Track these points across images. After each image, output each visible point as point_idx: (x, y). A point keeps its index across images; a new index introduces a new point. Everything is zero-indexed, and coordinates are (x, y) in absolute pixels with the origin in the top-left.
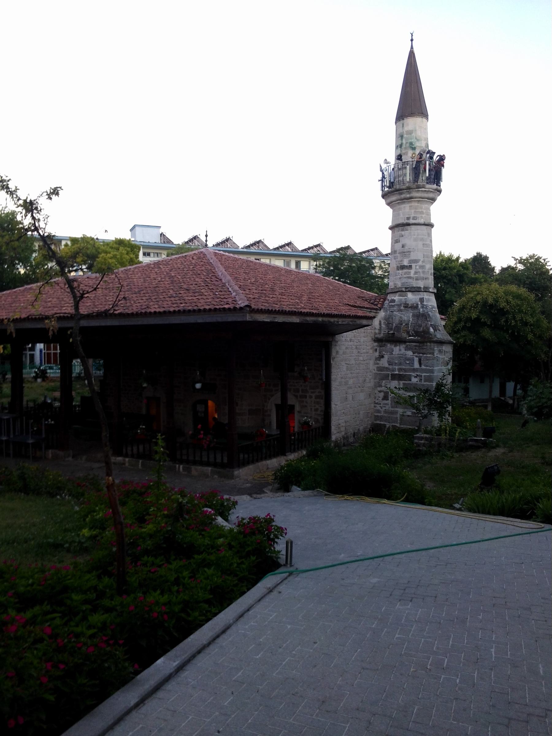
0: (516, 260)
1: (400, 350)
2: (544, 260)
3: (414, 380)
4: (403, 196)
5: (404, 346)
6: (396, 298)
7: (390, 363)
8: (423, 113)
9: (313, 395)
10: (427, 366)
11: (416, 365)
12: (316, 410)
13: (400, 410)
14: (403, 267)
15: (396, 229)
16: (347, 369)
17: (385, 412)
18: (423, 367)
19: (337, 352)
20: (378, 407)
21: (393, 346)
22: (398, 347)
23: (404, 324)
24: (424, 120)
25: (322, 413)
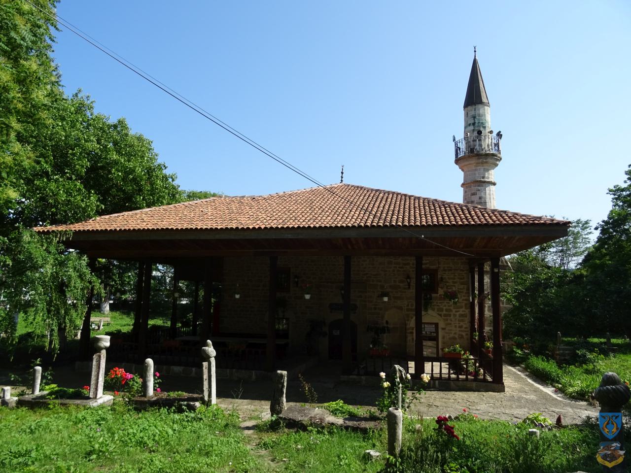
9: (458, 314)
12: (461, 327)
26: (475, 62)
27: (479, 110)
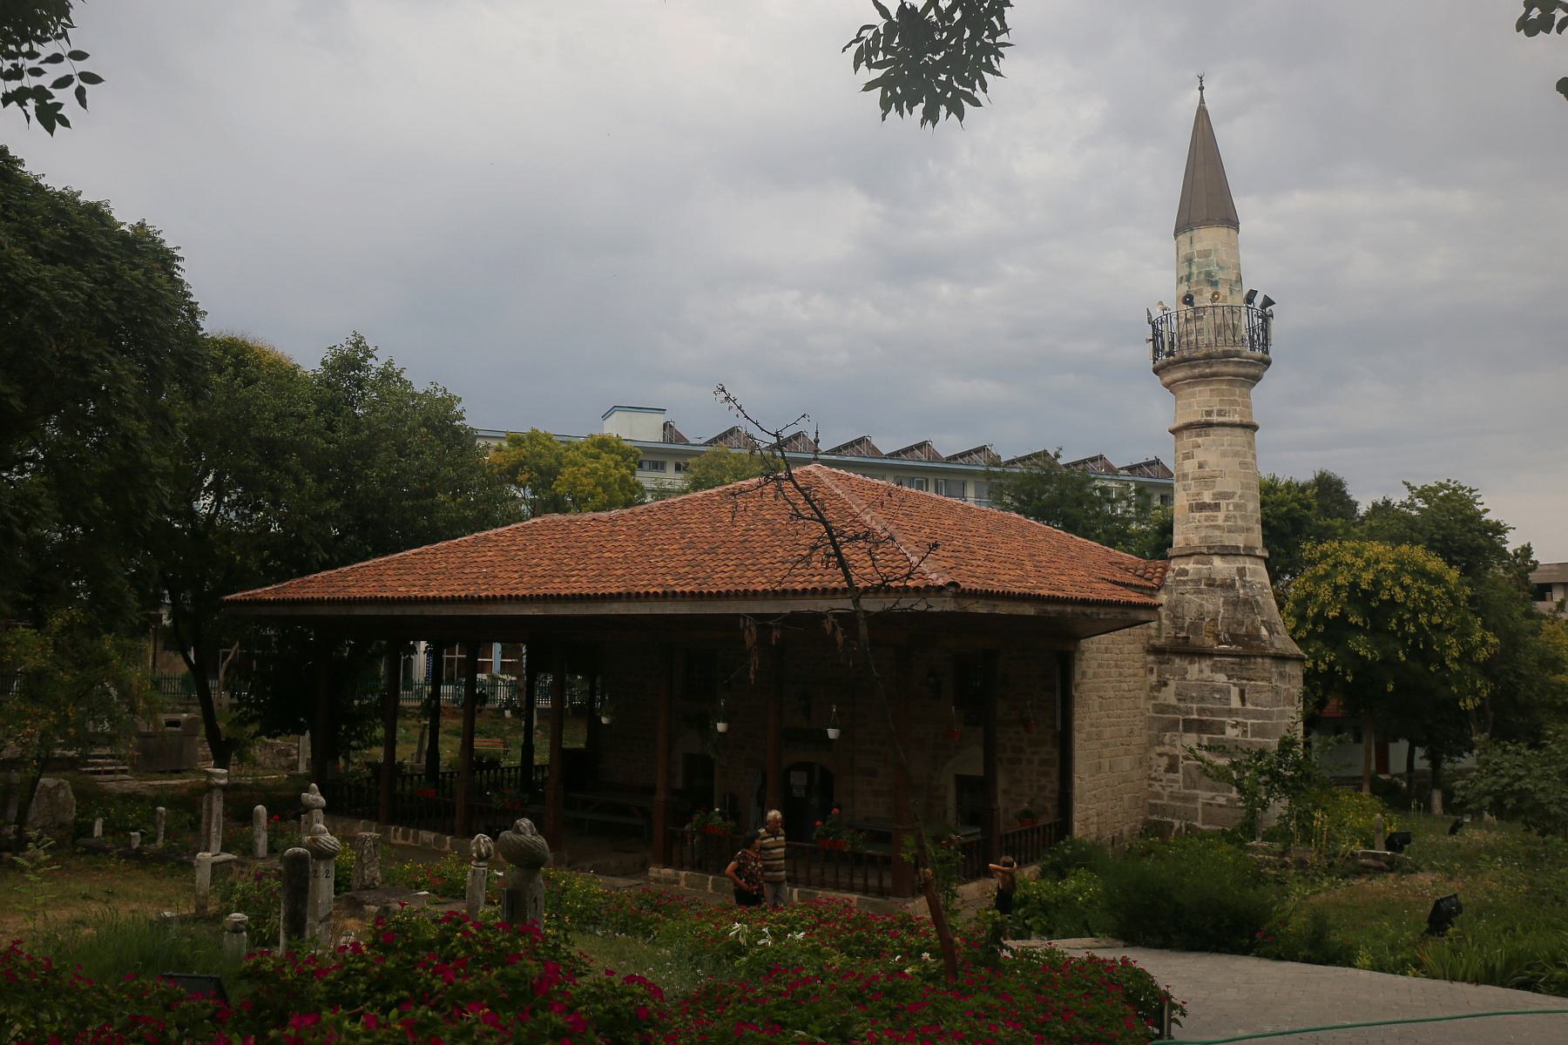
0: (1411, 488)
1: (1201, 671)
2: (1471, 491)
3: (1231, 733)
4: (1196, 371)
5: (1209, 662)
6: (1190, 566)
7: (1181, 697)
8: (1230, 221)
11: (1235, 702)
13: (1204, 795)
14: (1201, 507)
15: (1186, 433)
16: (1101, 708)
17: (1172, 796)
18: (1249, 706)
19: (1084, 674)
20: (1157, 787)
24: (1233, 232)
25: (1055, 796)
26: (1202, 113)
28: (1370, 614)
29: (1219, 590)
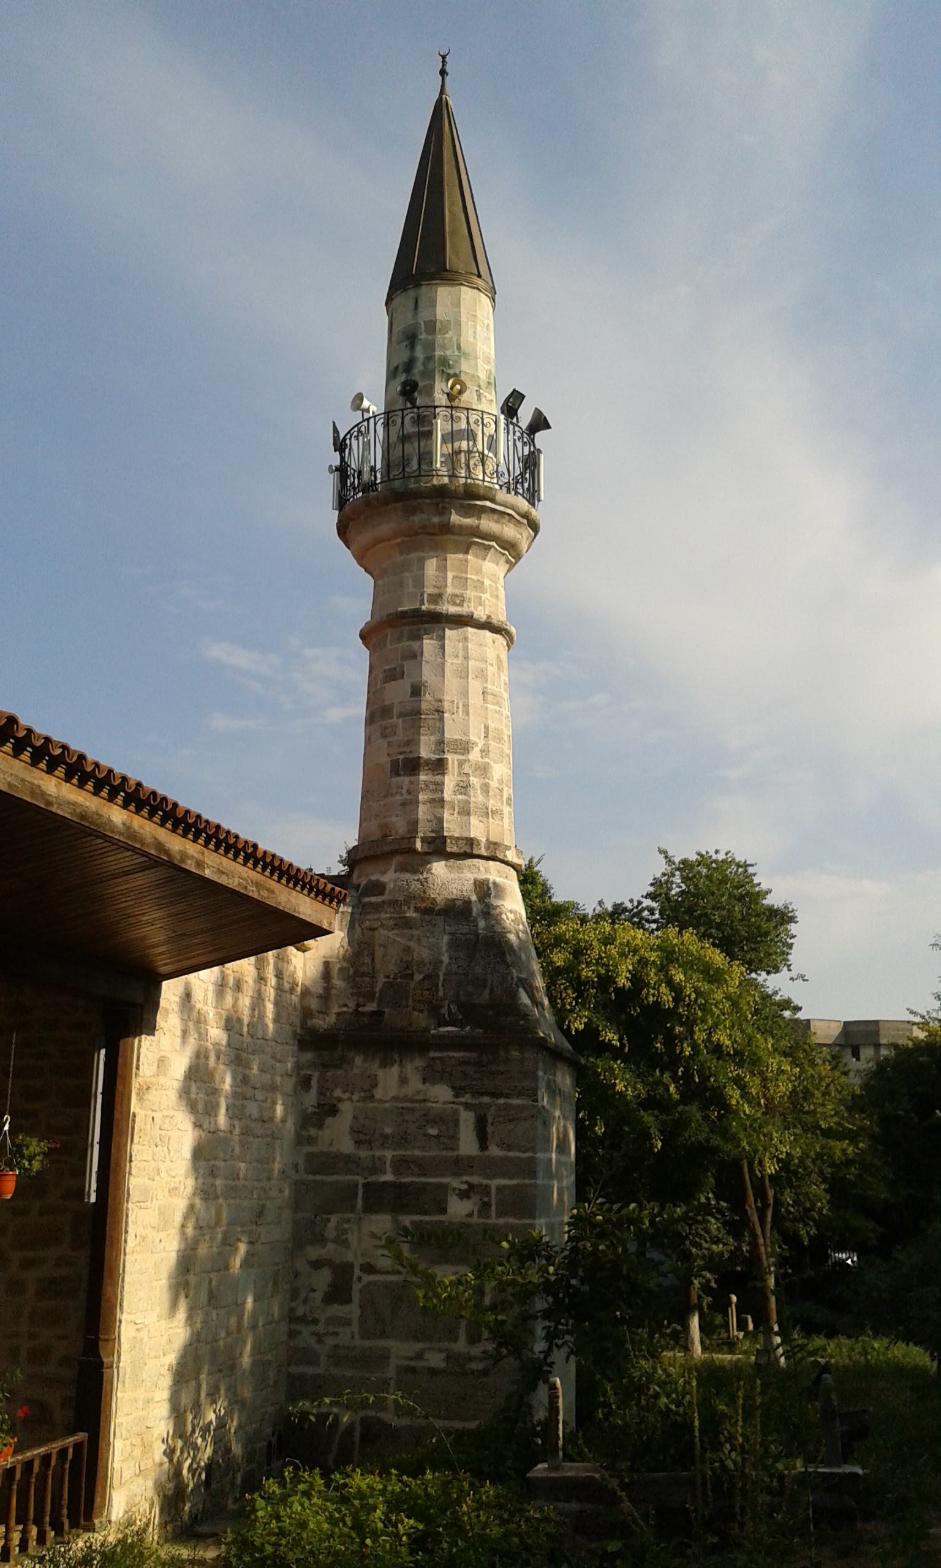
1: (403, 1081)
3: (459, 1209)
5: (419, 1063)
7: (362, 1136)
10: (510, 1148)
11: (467, 1144)
17: (338, 1357)
18: (494, 1151)
20: (306, 1336)
21: (374, 1067)
22: (395, 1070)
23: (418, 977)
26: (440, 112)
27: (433, 304)
28: (627, 1028)
29: (440, 921)
